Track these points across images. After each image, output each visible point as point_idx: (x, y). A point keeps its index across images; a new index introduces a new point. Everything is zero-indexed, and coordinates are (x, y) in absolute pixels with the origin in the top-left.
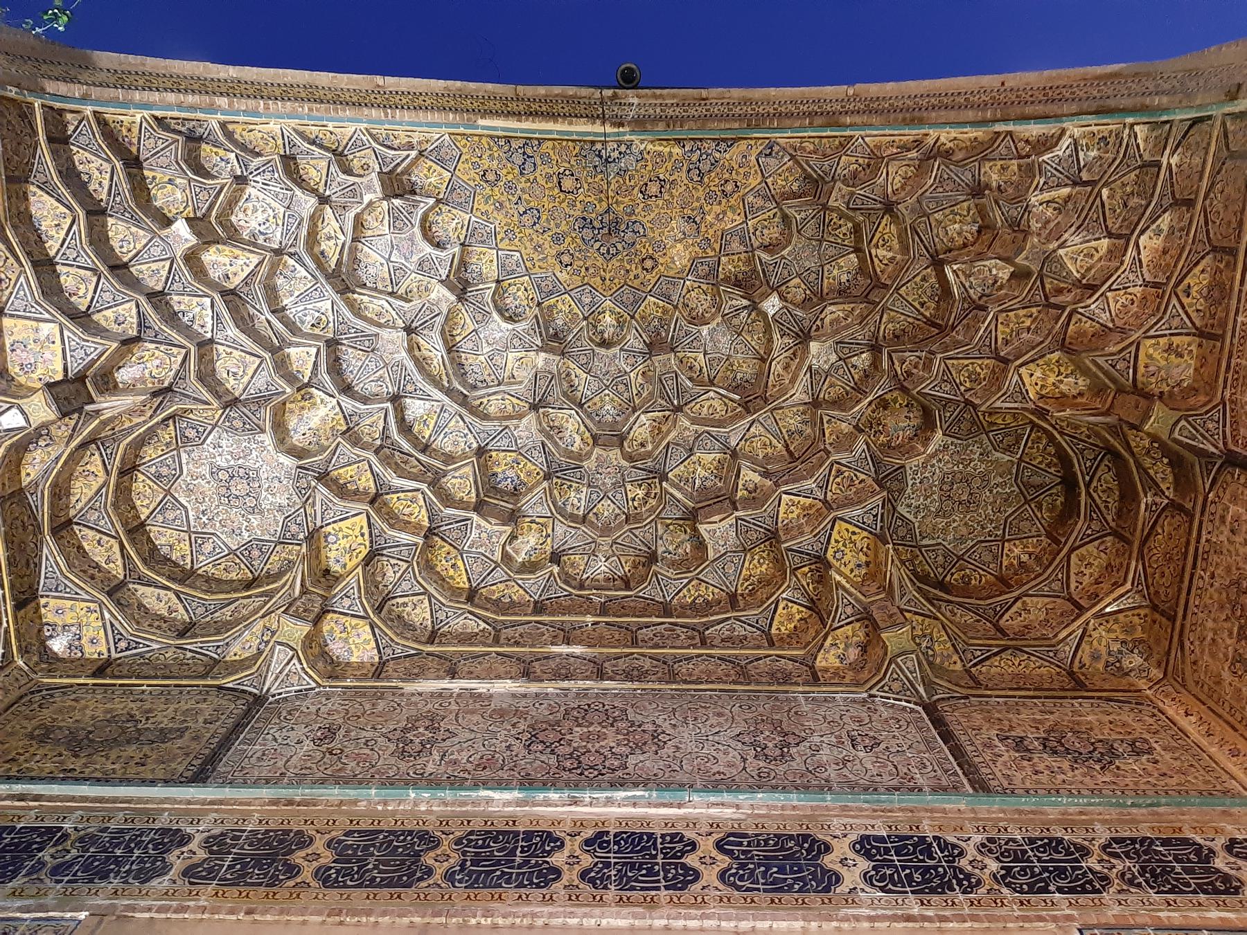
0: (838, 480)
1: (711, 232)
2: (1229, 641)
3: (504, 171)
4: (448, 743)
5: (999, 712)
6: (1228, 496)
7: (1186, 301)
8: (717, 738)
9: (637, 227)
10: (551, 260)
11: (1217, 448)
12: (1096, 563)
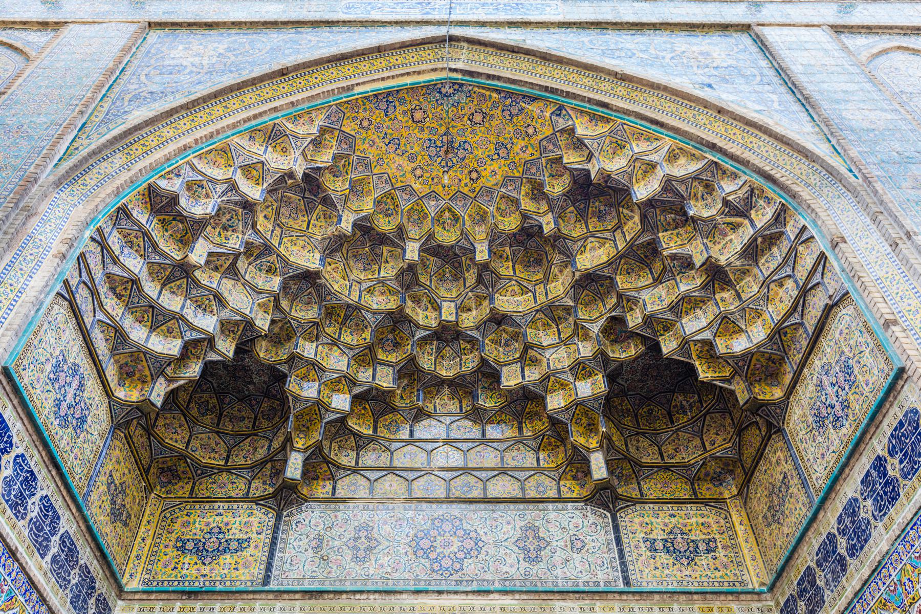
1: (517, 158)
4: (377, 550)
9: (467, 146)
10: (408, 175)
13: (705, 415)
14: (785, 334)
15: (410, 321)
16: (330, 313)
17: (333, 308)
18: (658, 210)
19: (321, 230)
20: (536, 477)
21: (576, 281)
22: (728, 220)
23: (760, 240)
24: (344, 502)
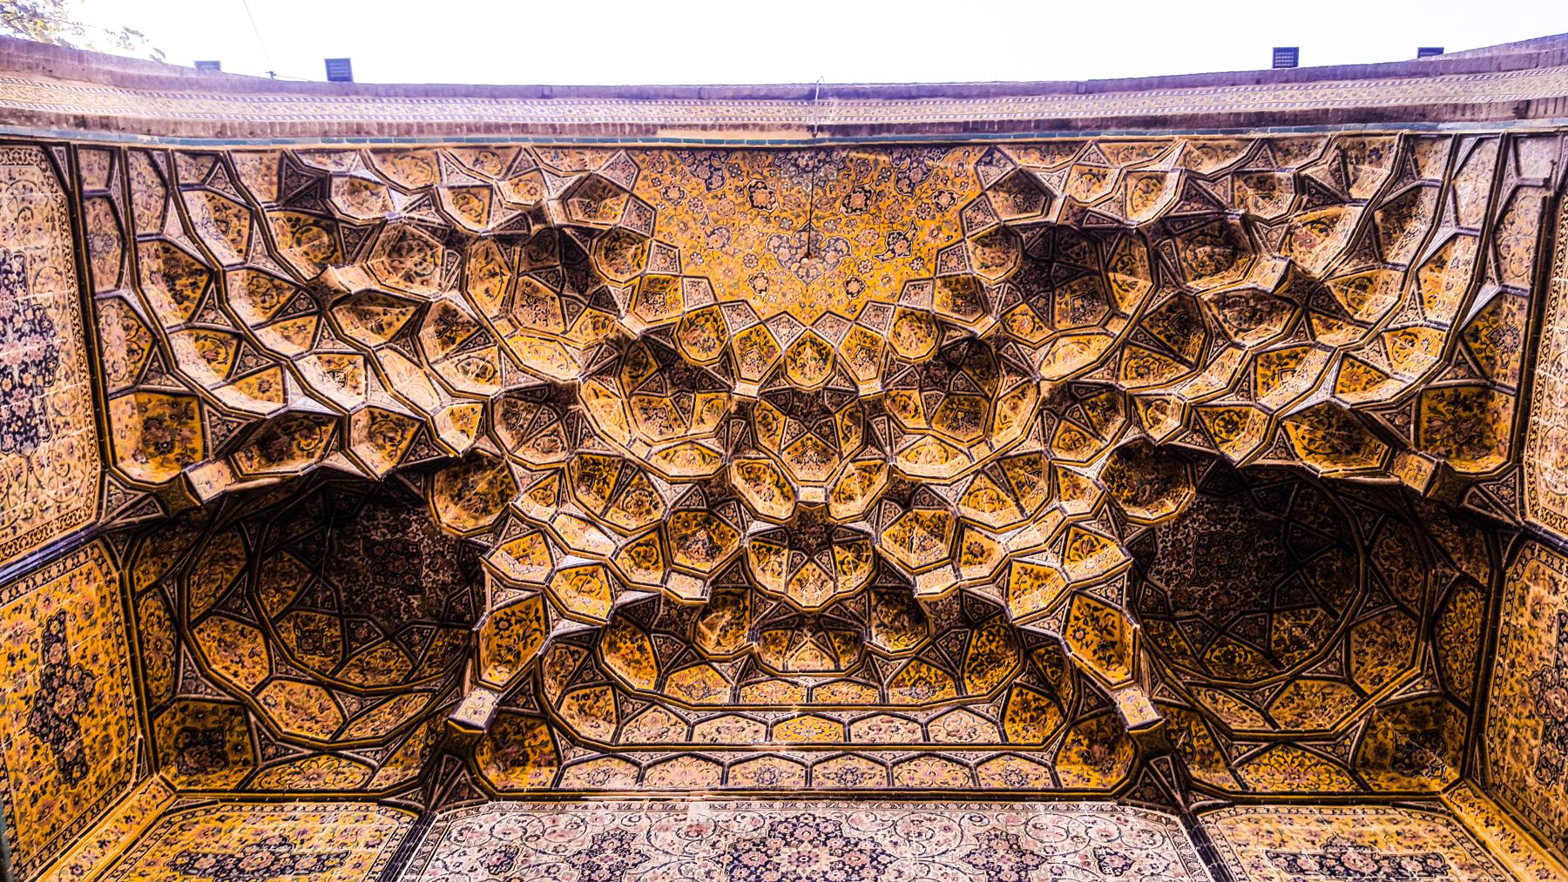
0: (1077, 544)
1: (925, 250)
2: (1533, 743)
3: (689, 187)
4: (640, 869)
5: (1269, 821)
6: (1527, 574)
7: (1475, 346)
8: (944, 859)
9: (841, 245)
11: (1513, 519)
12: (1379, 640)
13: (1347, 631)
14: (1475, 336)
15: (739, 502)
16: (590, 471)
17: (596, 463)
18: (1178, 240)
19: (583, 333)
20: (1000, 760)
21: (1044, 402)
22: (1312, 216)
23: (1378, 216)
24: (578, 798)
